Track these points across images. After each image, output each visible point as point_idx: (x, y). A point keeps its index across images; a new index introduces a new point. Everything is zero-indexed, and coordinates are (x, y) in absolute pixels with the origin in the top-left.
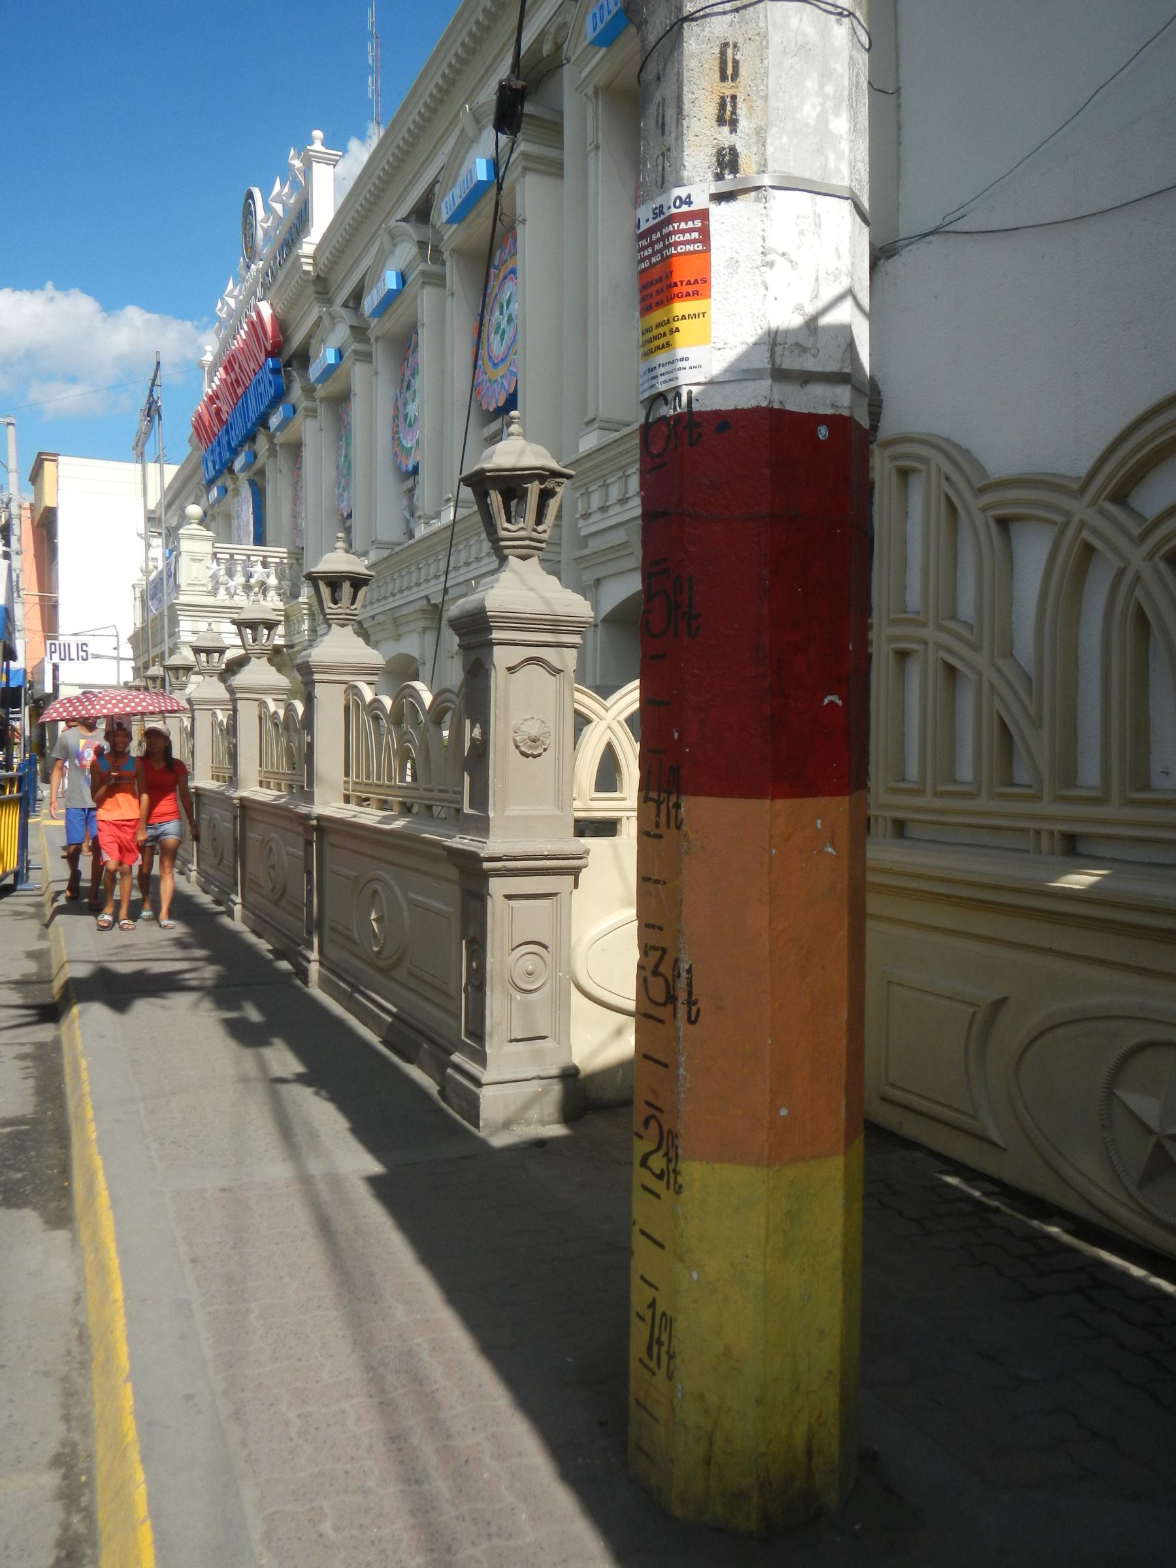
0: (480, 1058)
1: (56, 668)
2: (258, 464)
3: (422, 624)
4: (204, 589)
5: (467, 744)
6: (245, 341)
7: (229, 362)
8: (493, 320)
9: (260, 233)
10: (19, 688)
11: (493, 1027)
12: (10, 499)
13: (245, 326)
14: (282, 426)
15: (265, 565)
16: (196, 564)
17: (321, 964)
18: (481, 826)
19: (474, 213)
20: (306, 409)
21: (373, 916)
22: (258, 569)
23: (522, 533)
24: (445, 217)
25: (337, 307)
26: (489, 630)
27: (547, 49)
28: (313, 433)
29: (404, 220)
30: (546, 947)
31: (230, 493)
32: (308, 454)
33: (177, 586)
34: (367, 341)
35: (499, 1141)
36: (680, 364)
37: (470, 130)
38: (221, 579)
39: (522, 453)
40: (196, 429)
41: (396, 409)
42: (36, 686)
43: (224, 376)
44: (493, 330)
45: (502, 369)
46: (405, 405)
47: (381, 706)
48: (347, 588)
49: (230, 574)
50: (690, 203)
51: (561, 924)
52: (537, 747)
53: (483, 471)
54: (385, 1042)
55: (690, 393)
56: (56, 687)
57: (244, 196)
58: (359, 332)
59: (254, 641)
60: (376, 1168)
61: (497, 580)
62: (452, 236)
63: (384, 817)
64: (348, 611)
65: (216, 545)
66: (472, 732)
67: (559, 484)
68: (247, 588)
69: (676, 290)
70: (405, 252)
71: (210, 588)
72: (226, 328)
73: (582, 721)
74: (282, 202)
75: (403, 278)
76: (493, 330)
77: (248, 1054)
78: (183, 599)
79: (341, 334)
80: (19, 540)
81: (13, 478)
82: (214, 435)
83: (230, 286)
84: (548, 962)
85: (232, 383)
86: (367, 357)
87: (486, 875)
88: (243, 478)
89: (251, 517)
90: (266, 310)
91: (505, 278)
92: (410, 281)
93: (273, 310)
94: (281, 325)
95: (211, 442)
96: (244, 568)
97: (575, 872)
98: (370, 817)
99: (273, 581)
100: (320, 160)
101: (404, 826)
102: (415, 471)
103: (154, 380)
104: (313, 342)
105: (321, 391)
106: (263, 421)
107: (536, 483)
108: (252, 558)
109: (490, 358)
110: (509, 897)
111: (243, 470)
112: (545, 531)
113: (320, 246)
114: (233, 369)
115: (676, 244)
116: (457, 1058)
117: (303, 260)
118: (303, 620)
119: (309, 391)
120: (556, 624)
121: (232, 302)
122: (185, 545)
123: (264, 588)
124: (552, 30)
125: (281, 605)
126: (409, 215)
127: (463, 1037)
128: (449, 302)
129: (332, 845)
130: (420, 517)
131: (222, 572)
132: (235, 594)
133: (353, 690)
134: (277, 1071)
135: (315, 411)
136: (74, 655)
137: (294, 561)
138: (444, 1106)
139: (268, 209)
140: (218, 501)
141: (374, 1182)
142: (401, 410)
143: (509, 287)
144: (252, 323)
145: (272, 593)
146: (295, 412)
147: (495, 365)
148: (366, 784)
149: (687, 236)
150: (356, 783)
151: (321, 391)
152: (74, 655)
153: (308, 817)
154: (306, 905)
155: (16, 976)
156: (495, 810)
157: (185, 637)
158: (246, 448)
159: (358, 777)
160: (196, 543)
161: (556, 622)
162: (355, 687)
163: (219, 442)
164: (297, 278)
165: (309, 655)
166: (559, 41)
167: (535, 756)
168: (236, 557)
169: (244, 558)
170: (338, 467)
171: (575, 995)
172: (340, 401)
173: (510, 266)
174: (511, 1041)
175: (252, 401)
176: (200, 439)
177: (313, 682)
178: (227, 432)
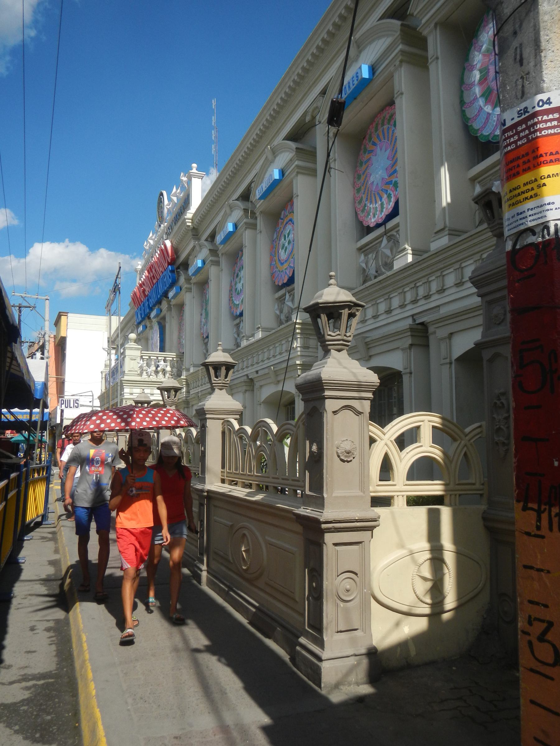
0: (321, 643)
1: (62, 411)
2: (162, 314)
3: (245, 388)
4: (136, 373)
5: (308, 455)
6: (158, 258)
7: (150, 268)
8: (281, 243)
9: (166, 210)
10: (46, 421)
11: (328, 624)
12: (45, 333)
14: (174, 297)
15: (165, 361)
16: (133, 361)
17: (208, 572)
18: (319, 502)
19: (271, 195)
20: (186, 288)
21: (243, 549)
22: (162, 363)
23: (339, 337)
24: (258, 196)
25: (203, 241)
26: (323, 390)
27: (308, 118)
28: (190, 300)
29: (236, 200)
30: (356, 574)
31: (148, 328)
32: (187, 309)
33: (124, 372)
34: (217, 256)
35: (336, 698)
36: (548, 207)
37: (270, 157)
38: (144, 369)
39: (338, 294)
40: (133, 299)
41: (231, 286)
42: (52, 420)
43: (147, 275)
44: (281, 248)
45: (286, 266)
46: (236, 284)
47: (245, 432)
48: (223, 370)
49: (148, 365)
50: (550, 103)
51: (365, 560)
52: (350, 456)
53: (317, 304)
54: (250, 623)
55: (556, 225)
56: (62, 420)
58: (214, 252)
59: (168, 398)
60: (266, 720)
61: (326, 363)
62: (260, 205)
63: (249, 493)
64: (224, 382)
66: (310, 448)
67: (358, 310)
68: (157, 372)
69: (542, 159)
70: (237, 214)
71: (139, 372)
72: (148, 253)
73: (372, 441)
74: (177, 196)
75: (236, 226)
76: (281, 248)
77: (175, 630)
78: (126, 378)
79: (205, 253)
80: (48, 352)
81: (47, 324)
82: (142, 301)
83: (151, 235)
84: (358, 583)
86: (217, 263)
87: (322, 532)
88: (155, 321)
89: (158, 339)
90: (168, 243)
91: (287, 223)
92: (238, 228)
93: (172, 244)
94: (175, 250)
95: (140, 305)
96: (155, 363)
97: (371, 529)
98: (240, 492)
99: (168, 369)
100: (196, 177)
101: (262, 499)
102: (241, 314)
104: (191, 257)
105: (194, 279)
106: (165, 294)
107: (347, 310)
108: (159, 358)
109: (279, 260)
110: (336, 545)
111: (155, 317)
112: (350, 336)
113: (195, 214)
114: (152, 271)
115: (540, 130)
116: (302, 640)
117: (187, 221)
119: (188, 280)
120: (359, 387)
121: (152, 242)
122: (128, 352)
123: (164, 372)
124: (311, 110)
126: (239, 198)
127: (306, 628)
128: (259, 236)
129: (215, 506)
130: (244, 337)
131: (145, 365)
132: (151, 375)
133: (227, 423)
134: (195, 644)
136: (72, 405)
137: (179, 359)
138: (295, 669)
139: (170, 200)
140: (142, 332)
141: (266, 729)
142: (234, 287)
143: (289, 227)
144: (162, 250)
146: (181, 290)
147: (282, 264)
148: (235, 474)
149: (549, 124)
150: (228, 473)
151: (194, 279)
152: (72, 405)
153: (202, 491)
154: (199, 538)
155: (44, 576)
156: (327, 493)
157: (126, 396)
158: (157, 307)
159: (230, 469)
160: (133, 352)
161: (359, 386)
162: (228, 421)
163: (144, 305)
164: (184, 229)
165: (204, 405)
166: (314, 116)
167: (348, 462)
168: (152, 357)
169: (155, 358)
171: (373, 603)
172: (203, 285)
173: (289, 218)
174: (338, 632)
175: (160, 285)
176: (135, 303)
177: (206, 419)
178: (148, 300)
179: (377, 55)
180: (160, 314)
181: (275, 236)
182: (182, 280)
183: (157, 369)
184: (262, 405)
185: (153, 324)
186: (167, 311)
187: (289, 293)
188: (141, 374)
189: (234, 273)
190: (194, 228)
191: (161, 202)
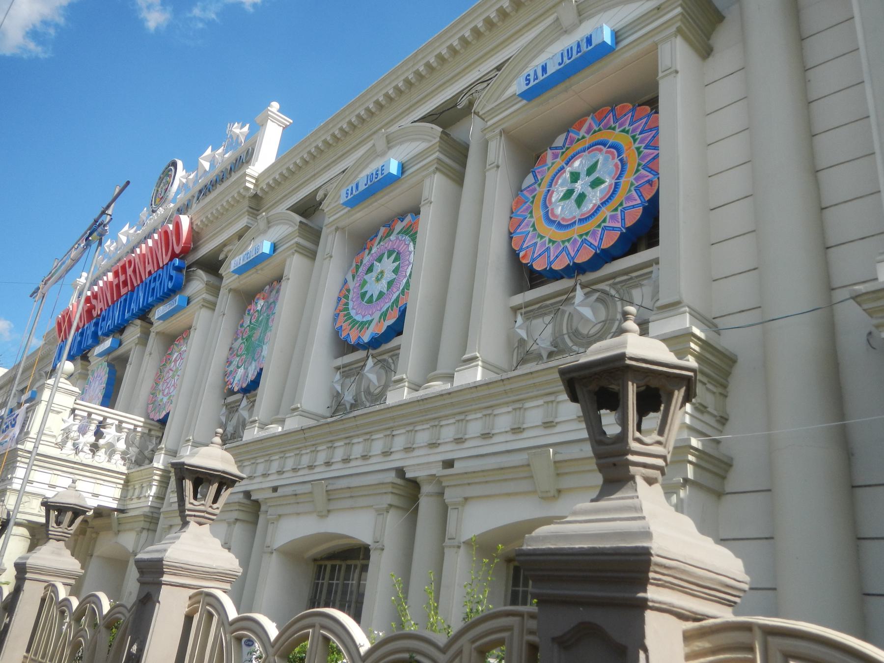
3: (389, 499)
4: (53, 440)
13: (156, 236)
14: (163, 318)
15: (119, 428)
38: (72, 435)
40: (59, 325)
57: (169, 161)
65: (78, 401)
68: (95, 448)
71: (59, 440)
83: (126, 228)
85: (118, 286)
93: (191, 223)
94: (195, 235)
99: (121, 446)
100: (275, 120)
103: (108, 207)
106: (144, 315)
108: (109, 421)
111: (101, 355)
117: (247, 178)
118: (150, 486)
121: (124, 239)
123: (111, 450)
125: (124, 469)
131: (75, 428)
132: (82, 451)
135: (215, 304)
137: (147, 431)
144: (166, 233)
145: (117, 457)
146: (188, 304)
170: (231, 349)
178: (96, 324)
179: (626, 20)
180: (116, 349)
181: (529, 179)
182: (198, 284)
183: (97, 440)
184: (462, 551)
185: (89, 368)
186: (136, 344)
187: (583, 287)
188: (61, 446)
189: (358, 267)
190: (256, 196)
191: (170, 176)
